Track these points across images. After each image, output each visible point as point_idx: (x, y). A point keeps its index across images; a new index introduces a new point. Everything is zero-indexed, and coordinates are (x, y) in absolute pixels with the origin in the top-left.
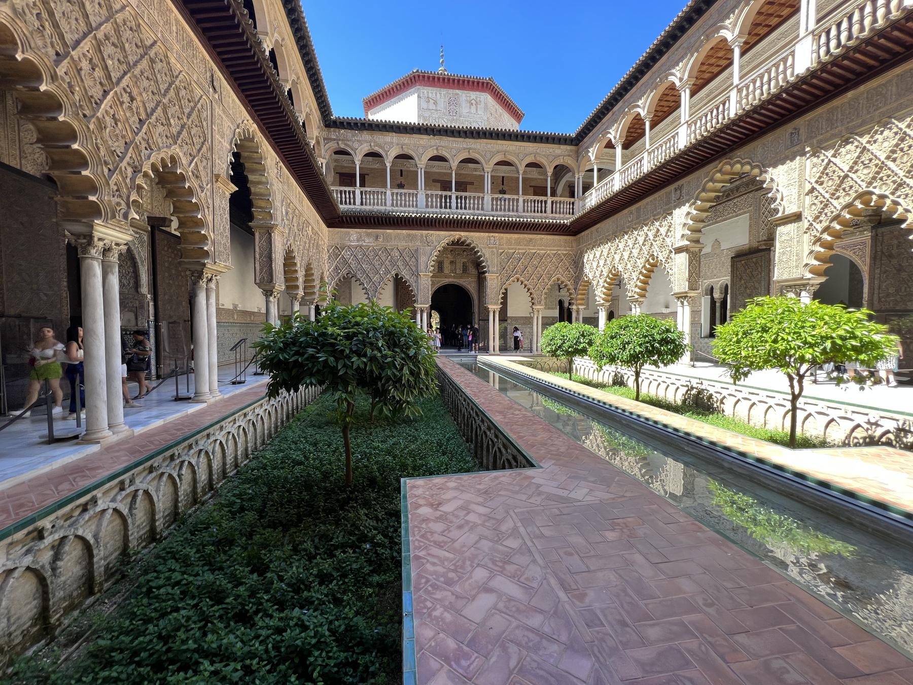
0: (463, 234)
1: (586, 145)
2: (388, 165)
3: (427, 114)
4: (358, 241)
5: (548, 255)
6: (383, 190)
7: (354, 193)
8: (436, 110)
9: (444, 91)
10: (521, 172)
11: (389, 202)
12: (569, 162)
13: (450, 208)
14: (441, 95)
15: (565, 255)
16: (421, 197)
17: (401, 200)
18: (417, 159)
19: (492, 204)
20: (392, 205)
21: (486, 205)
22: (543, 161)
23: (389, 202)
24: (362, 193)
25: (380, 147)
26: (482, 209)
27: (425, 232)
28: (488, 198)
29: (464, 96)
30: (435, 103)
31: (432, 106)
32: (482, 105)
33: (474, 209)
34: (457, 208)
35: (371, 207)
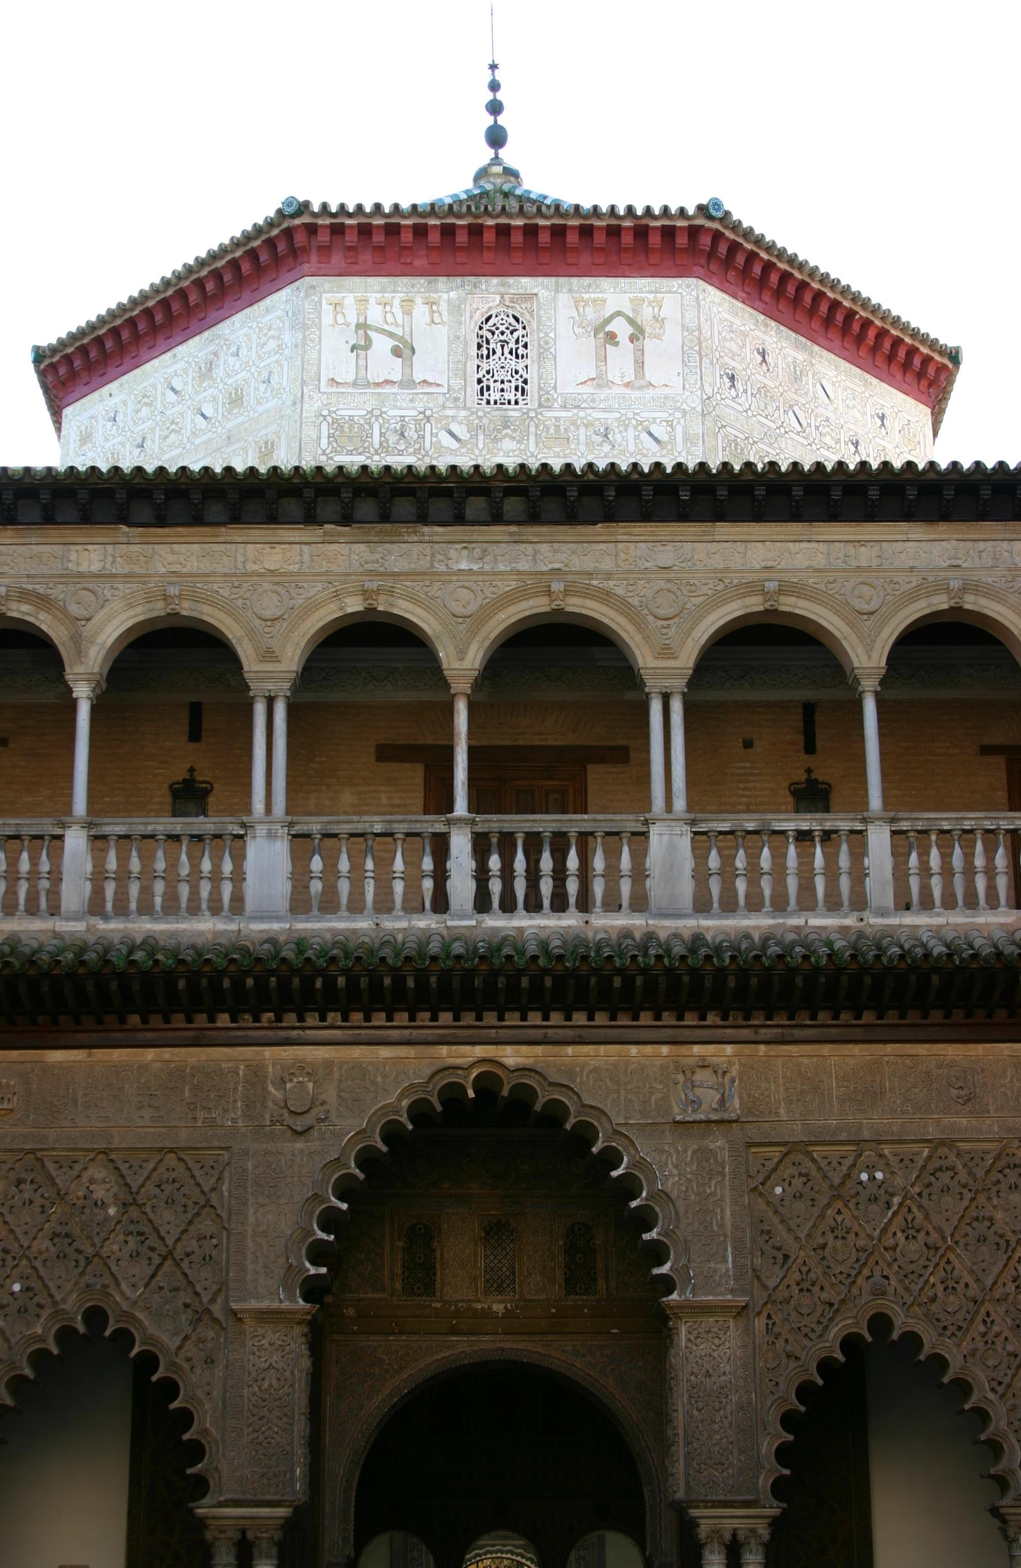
0: (511, 1056)
2: (83, 693)
3: (354, 408)
9: (448, 291)
10: (869, 685)
11: (74, 892)
13: (441, 903)
14: (435, 315)
16: (268, 860)
17: (147, 876)
18: (246, 652)
19: (701, 875)
20: (95, 907)
21: (668, 873)
23: (74, 892)
26: (640, 903)
27: (273, 1056)
28: (669, 846)
29: (563, 307)
30: (404, 350)
31: (382, 362)
32: (673, 335)
33: (584, 904)
34: (482, 903)
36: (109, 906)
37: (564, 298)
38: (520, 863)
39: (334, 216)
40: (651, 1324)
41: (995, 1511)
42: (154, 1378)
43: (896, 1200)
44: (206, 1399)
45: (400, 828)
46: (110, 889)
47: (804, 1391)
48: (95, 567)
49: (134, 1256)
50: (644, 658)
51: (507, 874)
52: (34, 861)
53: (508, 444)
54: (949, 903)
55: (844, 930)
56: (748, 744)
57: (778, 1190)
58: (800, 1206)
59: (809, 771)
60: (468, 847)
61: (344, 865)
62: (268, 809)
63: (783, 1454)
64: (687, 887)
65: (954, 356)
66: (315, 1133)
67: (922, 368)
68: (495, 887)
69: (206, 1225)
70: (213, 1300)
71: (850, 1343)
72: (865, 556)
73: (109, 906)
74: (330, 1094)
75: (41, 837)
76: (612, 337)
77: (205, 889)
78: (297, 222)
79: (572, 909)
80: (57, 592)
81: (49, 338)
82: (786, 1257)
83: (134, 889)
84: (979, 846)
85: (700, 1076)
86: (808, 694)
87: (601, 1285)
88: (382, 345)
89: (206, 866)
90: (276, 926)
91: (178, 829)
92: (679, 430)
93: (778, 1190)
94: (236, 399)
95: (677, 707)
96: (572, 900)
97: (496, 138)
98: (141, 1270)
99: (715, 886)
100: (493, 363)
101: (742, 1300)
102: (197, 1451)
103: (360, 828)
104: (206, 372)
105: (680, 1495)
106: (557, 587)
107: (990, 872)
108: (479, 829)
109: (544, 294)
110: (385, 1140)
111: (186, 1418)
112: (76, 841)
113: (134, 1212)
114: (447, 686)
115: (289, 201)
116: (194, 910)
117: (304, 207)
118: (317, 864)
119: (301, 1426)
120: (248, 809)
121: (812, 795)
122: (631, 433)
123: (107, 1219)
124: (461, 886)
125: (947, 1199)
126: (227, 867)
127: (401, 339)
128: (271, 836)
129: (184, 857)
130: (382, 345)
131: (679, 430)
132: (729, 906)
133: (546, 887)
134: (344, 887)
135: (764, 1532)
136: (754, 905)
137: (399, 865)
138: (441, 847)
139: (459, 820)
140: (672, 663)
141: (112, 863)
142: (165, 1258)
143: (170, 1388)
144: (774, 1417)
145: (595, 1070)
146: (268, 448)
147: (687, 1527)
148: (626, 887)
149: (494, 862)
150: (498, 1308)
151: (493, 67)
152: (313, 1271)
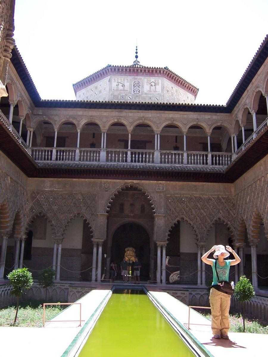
0: (135, 181)
1: (236, 112)
2: (79, 131)
4: (50, 187)
5: (210, 199)
6: (73, 149)
7: (52, 152)
8: (124, 90)
10: (185, 134)
11: (77, 158)
12: (226, 125)
13: (126, 161)
14: (127, 81)
15: (224, 198)
16: (103, 155)
18: (101, 126)
19: (161, 158)
20: (80, 160)
21: (157, 158)
22: (203, 125)
23: (77, 158)
24: (57, 152)
25: (74, 118)
26: (153, 162)
28: (157, 155)
30: (123, 86)
31: (120, 87)
33: (145, 162)
34: (132, 161)
35: (62, 162)
36: (82, 160)
37: (146, 80)
38: (137, 156)
39: (114, 67)
40: (151, 218)
41: (196, 244)
42: (87, 222)
43: (185, 203)
44: (93, 226)
45: (121, 151)
46: (82, 158)
47: (172, 227)
48: (81, 114)
49: (84, 206)
50: (155, 129)
51: (135, 157)
52: (72, 153)
53: (137, 99)
54: (194, 163)
55: (180, 166)
56: (168, 141)
57: (170, 201)
58: (172, 203)
59: (176, 145)
60: (130, 153)
61: (113, 155)
62: (103, 148)
63: (169, 235)
64: (159, 160)
65: (198, 90)
66: (108, 191)
67: (194, 91)
68: (134, 159)
69: (94, 202)
70: (95, 212)
71: (178, 221)
72: (185, 116)
73: (82, 160)
74: (111, 186)
75: (73, 150)
76: (152, 85)
77: (95, 158)
78: (109, 68)
79: (144, 162)
80: (76, 117)
81: (75, 83)
82: (170, 210)
83: (85, 158)
84: (199, 156)
85: (160, 185)
86: (177, 135)
87: (145, 212)
88: (120, 85)
89: (95, 155)
90: (104, 163)
91: (91, 150)
92: (160, 98)
93: (170, 201)
94: (100, 92)
95: (159, 136)
96: (144, 161)
97: (137, 57)
98: (85, 208)
99: (163, 160)
100: (135, 88)
101: (164, 215)
102: (92, 232)
103: (116, 150)
104: (96, 88)
105: (155, 240)
106: (143, 119)
107: (200, 159)
108: (132, 151)
109: (142, 78)
110: (118, 192)
111: (91, 228)
112: (78, 151)
113: (84, 200)
114: (128, 132)
115: (108, 65)
116: (93, 161)
117: (111, 65)
118: (110, 155)
119: (106, 229)
120: (101, 148)
121: (176, 148)
122: (154, 98)
123: (81, 201)
124: (129, 159)
125: (192, 203)
126: (98, 155)
127: (123, 84)
128: (104, 151)
129: (92, 154)
130: (120, 85)
131: (160, 98)
132: (165, 162)
133: (140, 159)
134: (113, 158)
135: (166, 245)
136: (168, 162)
137: (121, 156)
138: (126, 153)
139: (129, 150)
140: (159, 130)
141: (82, 154)
142: (88, 207)
143: (89, 224)
144: (168, 230)
145: (146, 184)
146: (105, 99)
147: (155, 244)
148: (151, 160)
149: (134, 156)
150: (132, 215)
151: (137, 47)
152: (108, 209)
